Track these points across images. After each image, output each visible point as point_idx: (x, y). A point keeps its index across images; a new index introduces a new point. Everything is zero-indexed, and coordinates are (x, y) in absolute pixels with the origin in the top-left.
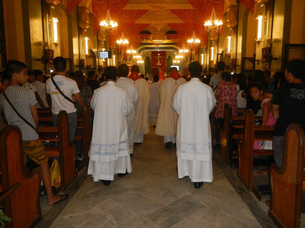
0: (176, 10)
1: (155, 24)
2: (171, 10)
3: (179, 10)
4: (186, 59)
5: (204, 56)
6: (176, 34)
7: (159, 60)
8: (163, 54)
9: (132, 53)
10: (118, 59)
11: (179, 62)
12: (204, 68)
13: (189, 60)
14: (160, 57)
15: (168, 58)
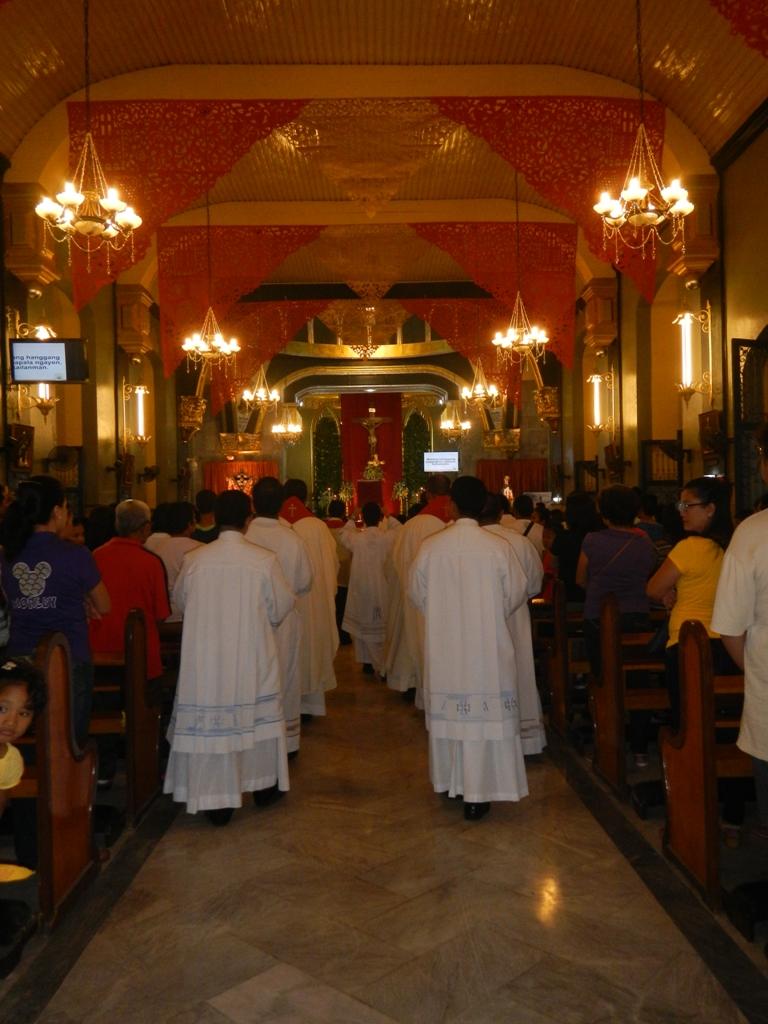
0: (465, 99)
1: (345, 181)
2: (435, 100)
3: (484, 100)
4: (486, 422)
5: (603, 385)
6: (447, 304)
7: (372, 431)
8: (389, 404)
9: (214, 350)
10: (179, 417)
11: (466, 426)
12: (609, 449)
13: (499, 425)
14: (378, 419)
15: (409, 422)
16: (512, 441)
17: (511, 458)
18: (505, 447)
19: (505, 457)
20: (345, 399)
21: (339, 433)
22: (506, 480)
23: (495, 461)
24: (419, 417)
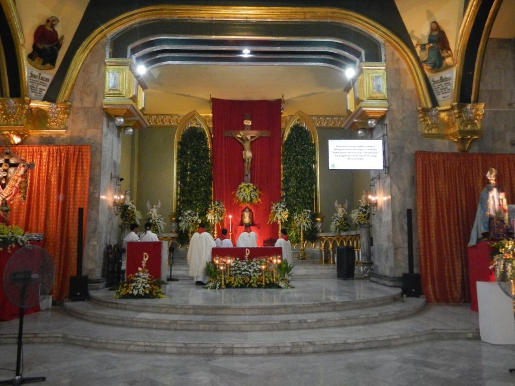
7: (247, 145)
8: (267, 112)
13: (447, 100)
14: (254, 133)
16: (471, 121)
17: (464, 152)
18: (460, 131)
19: (456, 149)
20: (218, 105)
21: (210, 147)
22: (491, 177)
23: (443, 154)
24: (302, 128)
